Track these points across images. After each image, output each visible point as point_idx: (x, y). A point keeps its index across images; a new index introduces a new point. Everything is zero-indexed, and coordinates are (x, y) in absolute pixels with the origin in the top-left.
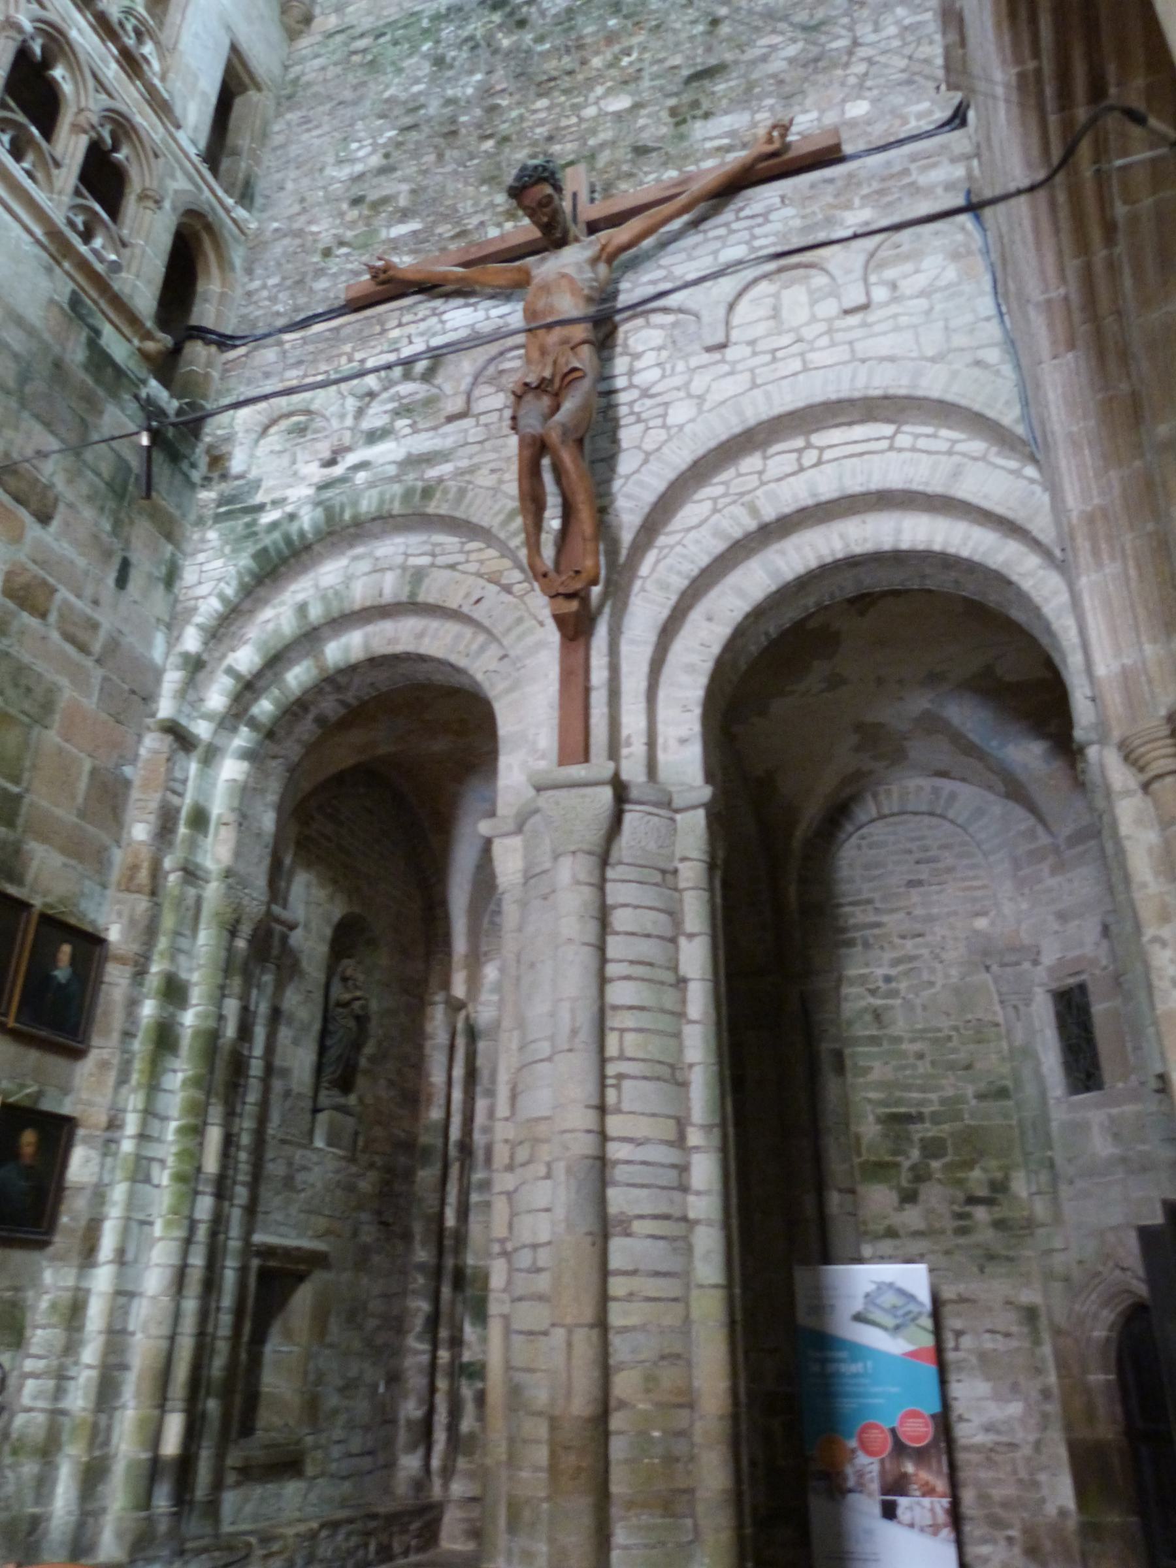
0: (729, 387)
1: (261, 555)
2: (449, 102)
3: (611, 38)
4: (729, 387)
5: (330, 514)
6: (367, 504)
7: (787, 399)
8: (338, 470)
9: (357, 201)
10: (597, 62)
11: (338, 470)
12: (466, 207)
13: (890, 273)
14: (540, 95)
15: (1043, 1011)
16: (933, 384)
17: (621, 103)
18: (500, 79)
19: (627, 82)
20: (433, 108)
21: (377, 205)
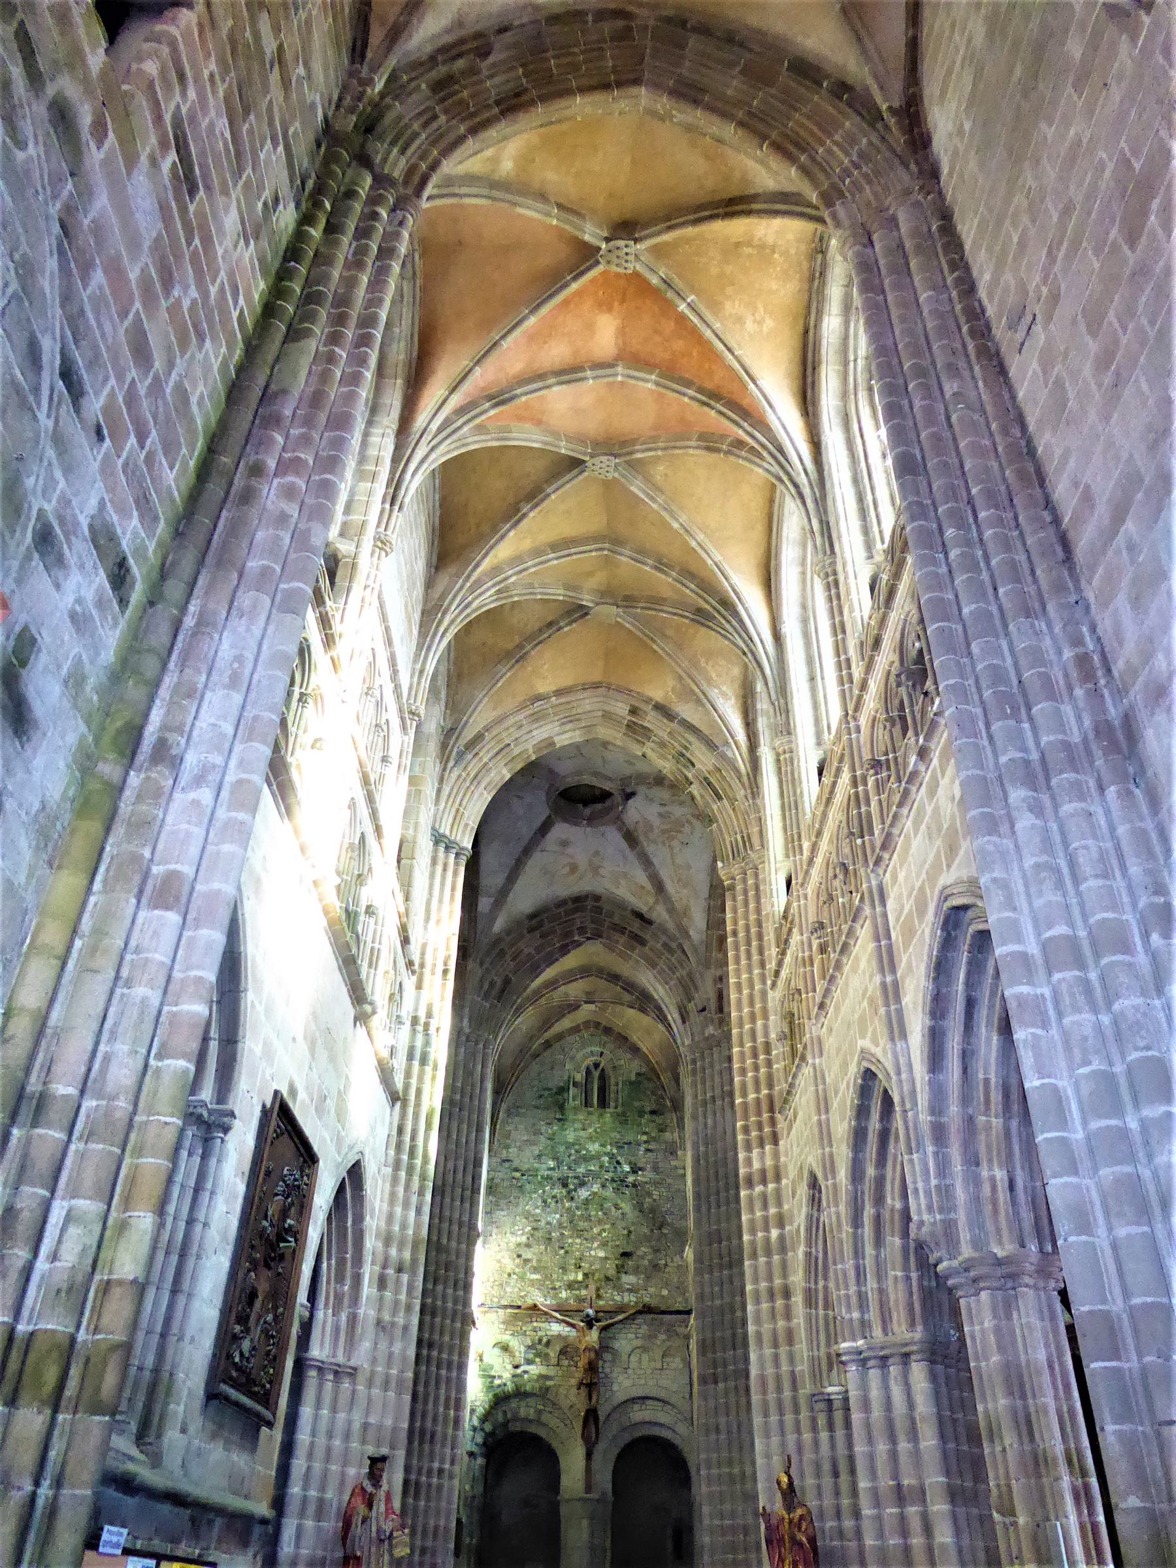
0: (627, 1383)
1: (495, 1395)
2: (548, 1223)
3: (600, 1222)
4: (627, 1383)
5: (517, 1388)
6: (528, 1388)
7: (641, 1393)
8: (519, 1371)
9: (519, 1256)
10: (595, 1231)
11: (519, 1371)
12: (555, 1276)
13: (667, 1359)
14: (579, 1237)
15: (669, 1532)
16: (673, 1400)
17: (601, 1254)
18: (565, 1218)
19: (604, 1245)
20: (543, 1223)
21: (526, 1261)
